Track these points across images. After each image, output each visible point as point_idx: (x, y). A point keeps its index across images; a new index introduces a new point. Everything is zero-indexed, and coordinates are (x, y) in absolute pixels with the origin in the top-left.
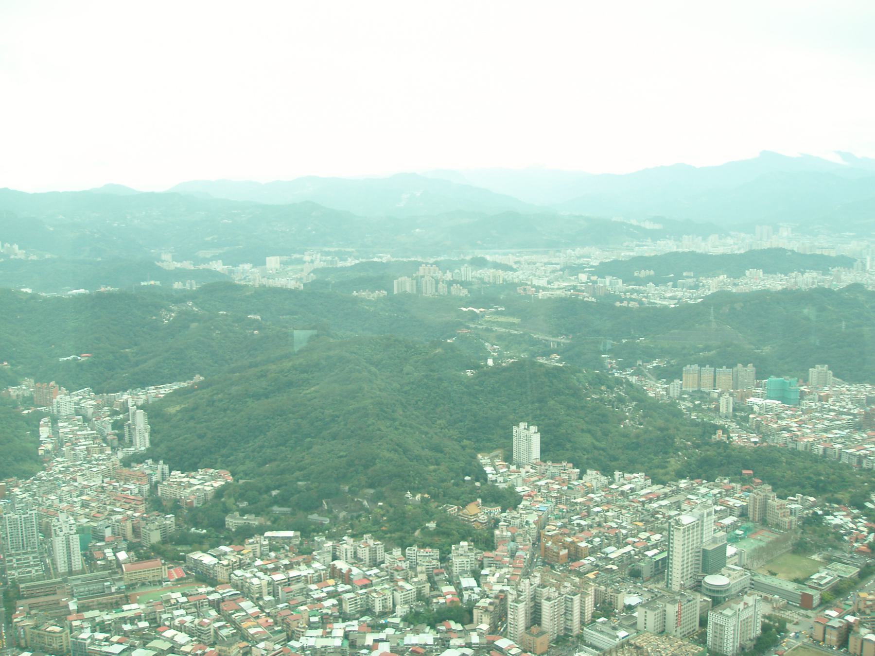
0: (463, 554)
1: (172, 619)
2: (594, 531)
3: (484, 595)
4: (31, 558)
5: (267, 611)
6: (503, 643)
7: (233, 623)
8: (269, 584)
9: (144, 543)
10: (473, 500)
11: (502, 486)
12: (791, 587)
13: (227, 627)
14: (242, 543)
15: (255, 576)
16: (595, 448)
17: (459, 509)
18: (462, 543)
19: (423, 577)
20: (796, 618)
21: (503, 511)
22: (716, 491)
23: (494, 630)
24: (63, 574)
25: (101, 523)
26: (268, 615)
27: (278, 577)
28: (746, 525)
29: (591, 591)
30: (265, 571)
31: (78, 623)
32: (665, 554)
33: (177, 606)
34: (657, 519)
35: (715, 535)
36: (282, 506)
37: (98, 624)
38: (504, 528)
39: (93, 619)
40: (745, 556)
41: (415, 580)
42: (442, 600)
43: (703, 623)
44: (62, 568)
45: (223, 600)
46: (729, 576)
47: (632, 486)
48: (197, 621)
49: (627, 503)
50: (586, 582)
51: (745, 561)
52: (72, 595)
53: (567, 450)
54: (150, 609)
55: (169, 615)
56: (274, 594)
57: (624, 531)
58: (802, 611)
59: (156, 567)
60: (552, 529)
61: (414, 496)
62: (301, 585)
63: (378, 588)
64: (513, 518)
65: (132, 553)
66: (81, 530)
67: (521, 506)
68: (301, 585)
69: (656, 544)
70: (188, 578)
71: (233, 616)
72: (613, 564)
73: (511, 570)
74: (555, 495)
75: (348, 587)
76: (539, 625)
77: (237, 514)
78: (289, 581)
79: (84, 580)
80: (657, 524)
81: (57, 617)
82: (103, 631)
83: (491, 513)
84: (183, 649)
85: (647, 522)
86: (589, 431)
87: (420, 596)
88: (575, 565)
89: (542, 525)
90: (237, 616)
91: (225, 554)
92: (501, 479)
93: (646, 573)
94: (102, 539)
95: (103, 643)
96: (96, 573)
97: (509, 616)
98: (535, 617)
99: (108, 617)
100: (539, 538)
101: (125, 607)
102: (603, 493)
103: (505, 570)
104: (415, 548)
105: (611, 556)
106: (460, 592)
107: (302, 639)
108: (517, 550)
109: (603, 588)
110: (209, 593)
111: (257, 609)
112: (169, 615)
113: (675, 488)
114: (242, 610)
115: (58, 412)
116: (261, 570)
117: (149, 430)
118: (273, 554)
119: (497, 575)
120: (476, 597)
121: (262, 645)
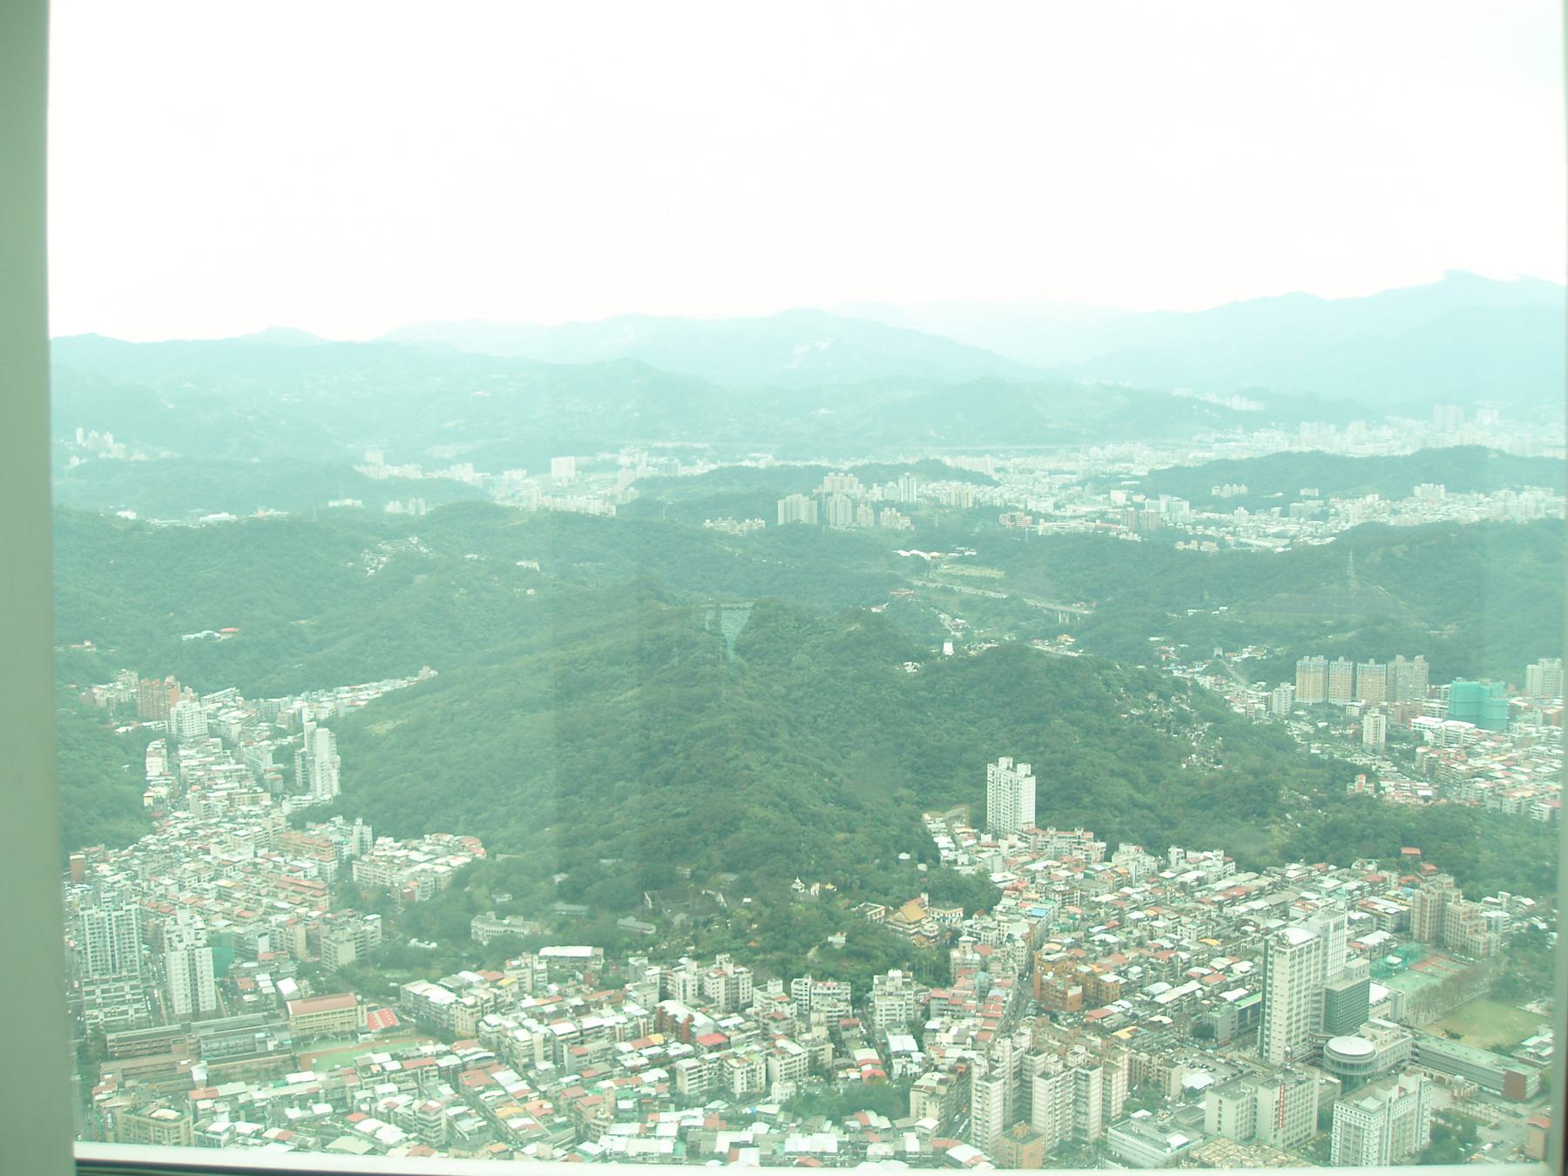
0: (893, 992)
1: (374, 1099)
2: (1131, 955)
3: (929, 1066)
4: (127, 988)
5: (542, 1088)
7: (482, 1109)
8: (546, 1040)
9: (327, 965)
10: (913, 896)
11: (966, 871)
12: (1485, 1060)
13: (470, 1116)
14: (499, 967)
15: (522, 1026)
16: (1136, 805)
17: (887, 911)
18: (892, 973)
19: (821, 1032)
20: (1495, 1116)
21: (968, 915)
22: (1353, 885)
23: (948, 1128)
24: (183, 1018)
25: (252, 927)
26: (544, 1095)
27: (564, 1027)
28: (1406, 947)
29: (1123, 1061)
30: (540, 1017)
31: (207, 1104)
32: (1257, 998)
33: (383, 1076)
34: (1245, 933)
35: (1349, 965)
36: (572, 901)
37: (243, 1106)
38: (969, 947)
39: (235, 1097)
40: (1403, 1003)
41: (807, 1037)
42: (854, 1075)
43: (1325, 1122)
44: (182, 1006)
45: (464, 1067)
46: (1374, 1038)
47: (1200, 874)
48: (417, 1104)
49: (1190, 905)
50: (1114, 1046)
51: (1404, 1012)
52: (198, 1055)
53: (1085, 808)
54: (333, 1083)
55: (369, 1094)
56: (556, 1058)
57: (1185, 956)
58: (1506, 1105)
59: (348, 1008)
60: (1055, 949)
61: (808, 887)
62: (603, 1043)
63: (740, 1051)
64: (984, 928)
65: (305, 982)
66: (215, 941)
67: (999, 908)
68: (603, 1043)
69: (1242, 979)
70: (403, 1028)
71: (482, 1097)
72: (1164, 1014)
73: (979, 1021)
74: (1062, 888)
75: (687, 1048)
76: (1029, 1122)
77: (492, 914)
78: (582, 1037)
79: (219, 1028)
80: (1245, 944)
81: (171, 1093)
82: (250, 1118)
83: (944, 919)
85: (1227, 939)
86: (1124, 774)
87: (815, 1067)
88: (1094, 1015)
89: (1036, 942)
90: (489, 1097)
91: (470, 985)
92: (964, 859)
93: (1224, 1029)
94: (253, 956)
95: (251, 1141)
96: (241, 1017)
97: (974, 1105)
98: (1021, 1107)
99: (259, 1094)
100: (1030, 967)
101: (291, 1078)
102: (1148, 887)
103: (968, 1022)
104: (808, 980)
105: (1160, 999)
106: (886, 1061)
107: (604, 1139)
108: (991, 985)
109: (1144, 1057)
110: (439, 1055)
111: (524, 1085)
112: (369, 1094)
113: (1278, 878)
114: (498, 1086)
115: (180, 730)
116: (533, 1016)
117: (338, 765)
118: (554, 988)
119: (954, 1031)
120: (916, 1069)
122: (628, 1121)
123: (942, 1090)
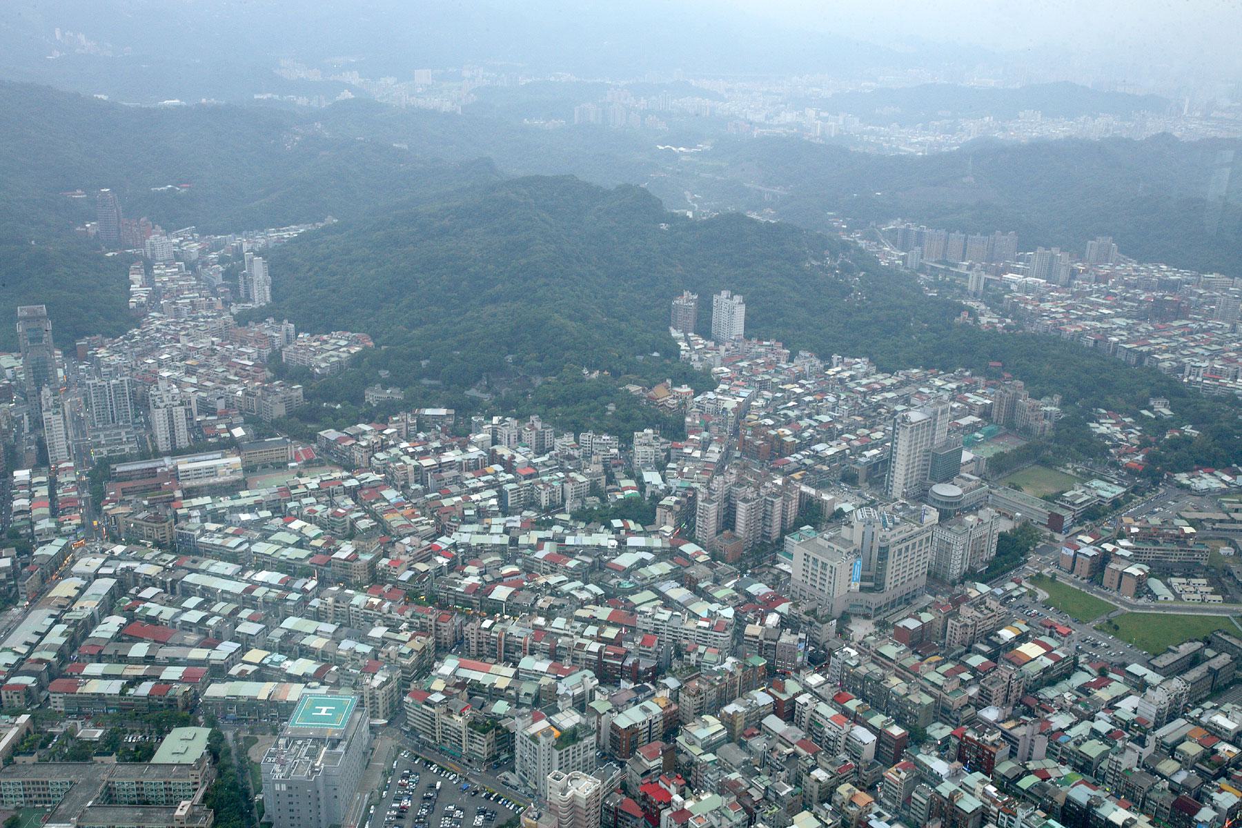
0: (646, 442)
3: (668, 492)
5: (414, 501)
6: (689, 548)
11: (698, 366)
14: (385, 422)
19: (600, 468)
27: (428, 462)
29: (795, 495)
30: (412, 455)
34: (880, 414)
36: (433, 378)
39: (202, 507)
42: (620, 496)
45: (361, 487)
56: (422, 481)
57: (839, 427)
62: (454, 472)
63: (546, 478)
68: (454, 472)
75: (510, 476)
76: (733, 530)
78: (441, 467)
84: (313, 543)
87: (594, 490)
91: (364, 433)
98: (728, 520)
101: (243, 493)
106: (642, 486)
107: (455, 535)
110: (344, 479)
112: (297, 504)
114: (385, 500)
115: (153, 255)
118: (421, 435)
121: (407, 540)
122: (471, 523)
123: (678, 508)
